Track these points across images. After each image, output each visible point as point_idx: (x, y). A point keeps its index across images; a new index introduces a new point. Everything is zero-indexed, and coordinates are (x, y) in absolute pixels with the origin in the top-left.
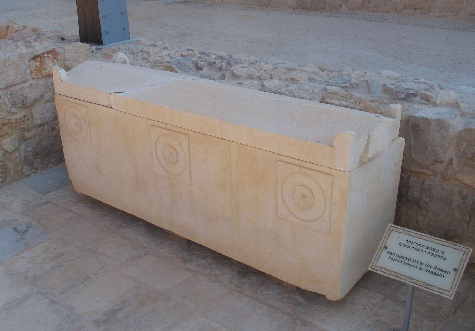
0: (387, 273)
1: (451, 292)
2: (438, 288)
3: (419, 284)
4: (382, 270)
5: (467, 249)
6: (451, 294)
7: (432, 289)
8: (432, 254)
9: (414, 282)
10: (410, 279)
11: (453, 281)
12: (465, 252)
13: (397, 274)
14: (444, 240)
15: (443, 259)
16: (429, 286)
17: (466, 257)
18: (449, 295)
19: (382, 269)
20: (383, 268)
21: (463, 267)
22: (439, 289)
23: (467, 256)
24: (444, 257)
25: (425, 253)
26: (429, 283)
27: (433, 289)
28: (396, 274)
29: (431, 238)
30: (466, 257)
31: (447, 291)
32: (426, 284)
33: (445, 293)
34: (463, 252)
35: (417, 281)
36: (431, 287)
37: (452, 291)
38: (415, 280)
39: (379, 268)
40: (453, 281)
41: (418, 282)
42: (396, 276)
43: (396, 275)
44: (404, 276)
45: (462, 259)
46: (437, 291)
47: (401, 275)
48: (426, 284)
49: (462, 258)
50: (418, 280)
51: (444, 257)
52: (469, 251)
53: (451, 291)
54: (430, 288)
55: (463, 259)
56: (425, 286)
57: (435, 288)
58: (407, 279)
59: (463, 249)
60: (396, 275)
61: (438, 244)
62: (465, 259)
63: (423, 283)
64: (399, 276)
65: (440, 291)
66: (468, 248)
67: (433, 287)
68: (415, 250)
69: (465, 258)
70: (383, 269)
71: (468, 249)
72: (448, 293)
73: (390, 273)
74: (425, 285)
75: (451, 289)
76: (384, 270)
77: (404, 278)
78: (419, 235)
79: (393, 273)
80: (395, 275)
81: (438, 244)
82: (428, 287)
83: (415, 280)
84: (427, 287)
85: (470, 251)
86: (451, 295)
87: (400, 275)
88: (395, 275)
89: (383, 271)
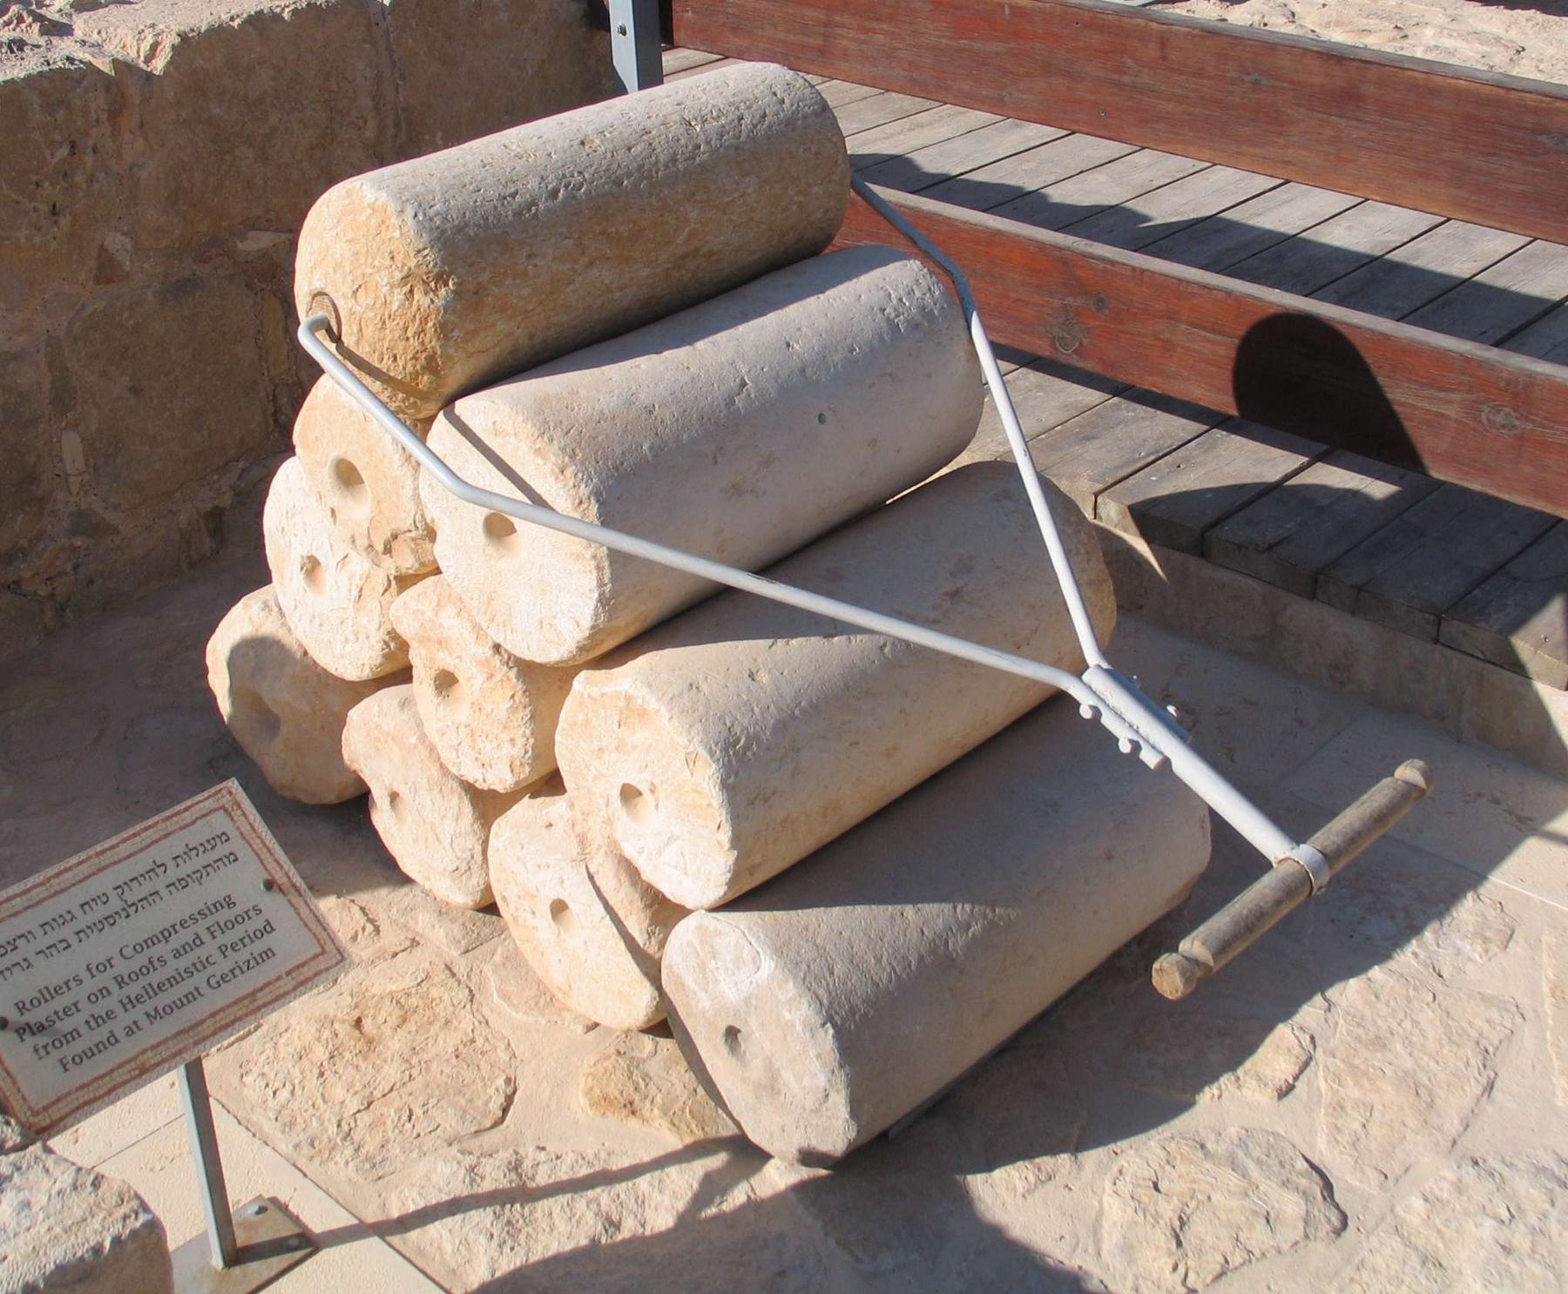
0: (102, 1092)
1: (329, 947)
2: (288, 973)
3: (227, 1020)
4: (76, 1104)
5: (220, 796)
6: (335, 951)
7: (277, 993)
8: (183, 879)
9: (210, 1032)
10: (186, 1035)
11: (299, 914)
12: (226, 810)
13: (133, 1065)
14: (131, 831)
15: (227, 862)
16: (259, 995)
17: (246, 818)
18: (335, 961)
19: (69, 1099)
20: (69, 1094)
21: (272, 854)
22: (294, 974)
23: (244, 814)
24: (226, 857)
25: (161, 899)
26: (251, 989)
27: (281, 991)
28: (128, 1067)
29: (90, 858)
30: (246, 818)
31: (315, 957)
32: (245, 997)
33: (322, 967)
34: (222, 811)
35: (212, 1020)
36: (267, 990)
37: (329, 942)
38: (202, 1022)
39: (55, 1108)
40: (299, 914)
41: (218, 1017)
42: (137, 1072)
43: (134, 1070)
44: (162, 1047)
45: (242, 834)
46: (294, 983)
47: (149, 1053)
48: (246, 1002)
49: (238, 828)
50: (213, 1015)
51: (226, 857)
52: (230, 793)
53: (325, 947)
54: (269, 998)
55: (246, 833)
56: (251, 1007)
57: (281, 983)
58: (181, 1045)
59: (210, 804)
60: (134, 1070)
61: (129, 857)
62: (249, 827)
63: (235, 1008)
64: (148, 1065)
65: (302, 978)
66: (221, 790)
67: (271, 987)
68: (94, 936)
69: (245, 822)
70: (74, 1096)
71: (224, 792)
72: (326, 956)
73: (110, 1085)
74: (247, 1007)
75: (319, 940)
76: (80, 1093)
77: (169, 1053)
78: (43, 888)
79: (116, 1074)
80: (133, 1073)
81: (129, 857)
82: (260, 1002)
83: (202, 1022)
84: (256, 1004)
85: (233, 791)
86: (339, 957)
87: (145, 1057)
88: (129, 1072)
89: (81, 1101)
